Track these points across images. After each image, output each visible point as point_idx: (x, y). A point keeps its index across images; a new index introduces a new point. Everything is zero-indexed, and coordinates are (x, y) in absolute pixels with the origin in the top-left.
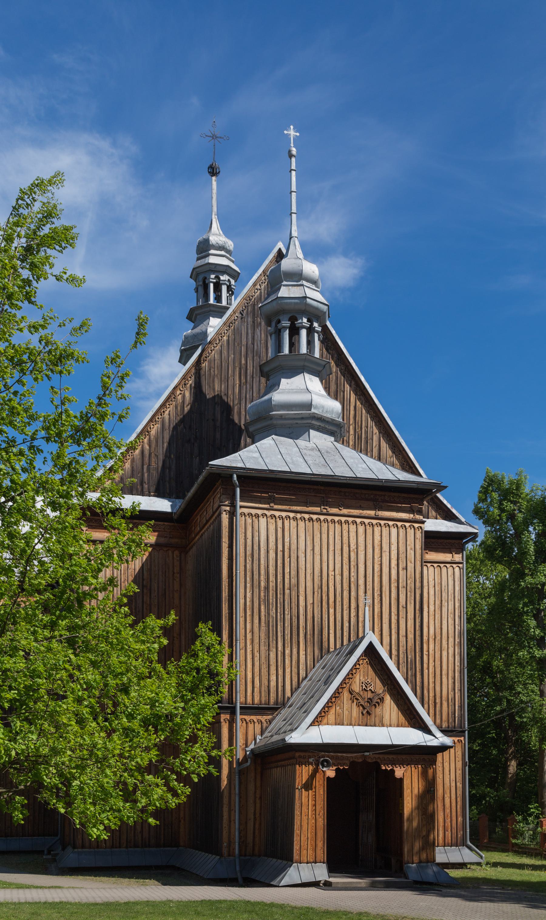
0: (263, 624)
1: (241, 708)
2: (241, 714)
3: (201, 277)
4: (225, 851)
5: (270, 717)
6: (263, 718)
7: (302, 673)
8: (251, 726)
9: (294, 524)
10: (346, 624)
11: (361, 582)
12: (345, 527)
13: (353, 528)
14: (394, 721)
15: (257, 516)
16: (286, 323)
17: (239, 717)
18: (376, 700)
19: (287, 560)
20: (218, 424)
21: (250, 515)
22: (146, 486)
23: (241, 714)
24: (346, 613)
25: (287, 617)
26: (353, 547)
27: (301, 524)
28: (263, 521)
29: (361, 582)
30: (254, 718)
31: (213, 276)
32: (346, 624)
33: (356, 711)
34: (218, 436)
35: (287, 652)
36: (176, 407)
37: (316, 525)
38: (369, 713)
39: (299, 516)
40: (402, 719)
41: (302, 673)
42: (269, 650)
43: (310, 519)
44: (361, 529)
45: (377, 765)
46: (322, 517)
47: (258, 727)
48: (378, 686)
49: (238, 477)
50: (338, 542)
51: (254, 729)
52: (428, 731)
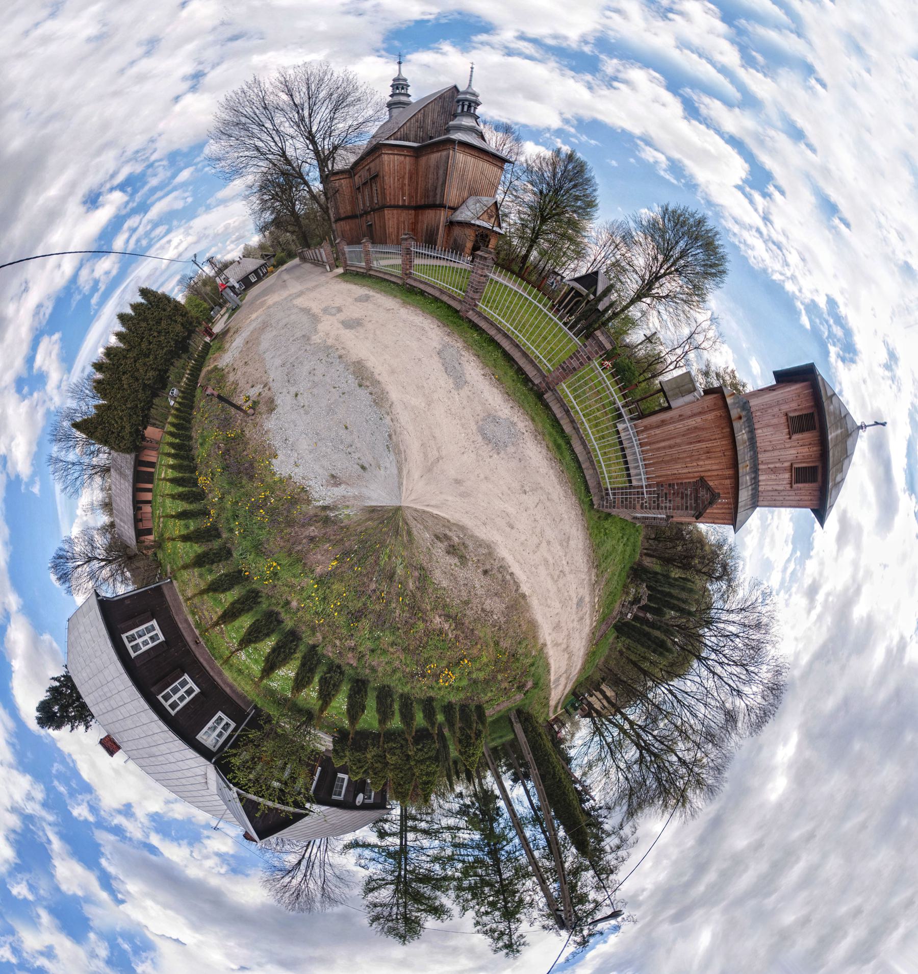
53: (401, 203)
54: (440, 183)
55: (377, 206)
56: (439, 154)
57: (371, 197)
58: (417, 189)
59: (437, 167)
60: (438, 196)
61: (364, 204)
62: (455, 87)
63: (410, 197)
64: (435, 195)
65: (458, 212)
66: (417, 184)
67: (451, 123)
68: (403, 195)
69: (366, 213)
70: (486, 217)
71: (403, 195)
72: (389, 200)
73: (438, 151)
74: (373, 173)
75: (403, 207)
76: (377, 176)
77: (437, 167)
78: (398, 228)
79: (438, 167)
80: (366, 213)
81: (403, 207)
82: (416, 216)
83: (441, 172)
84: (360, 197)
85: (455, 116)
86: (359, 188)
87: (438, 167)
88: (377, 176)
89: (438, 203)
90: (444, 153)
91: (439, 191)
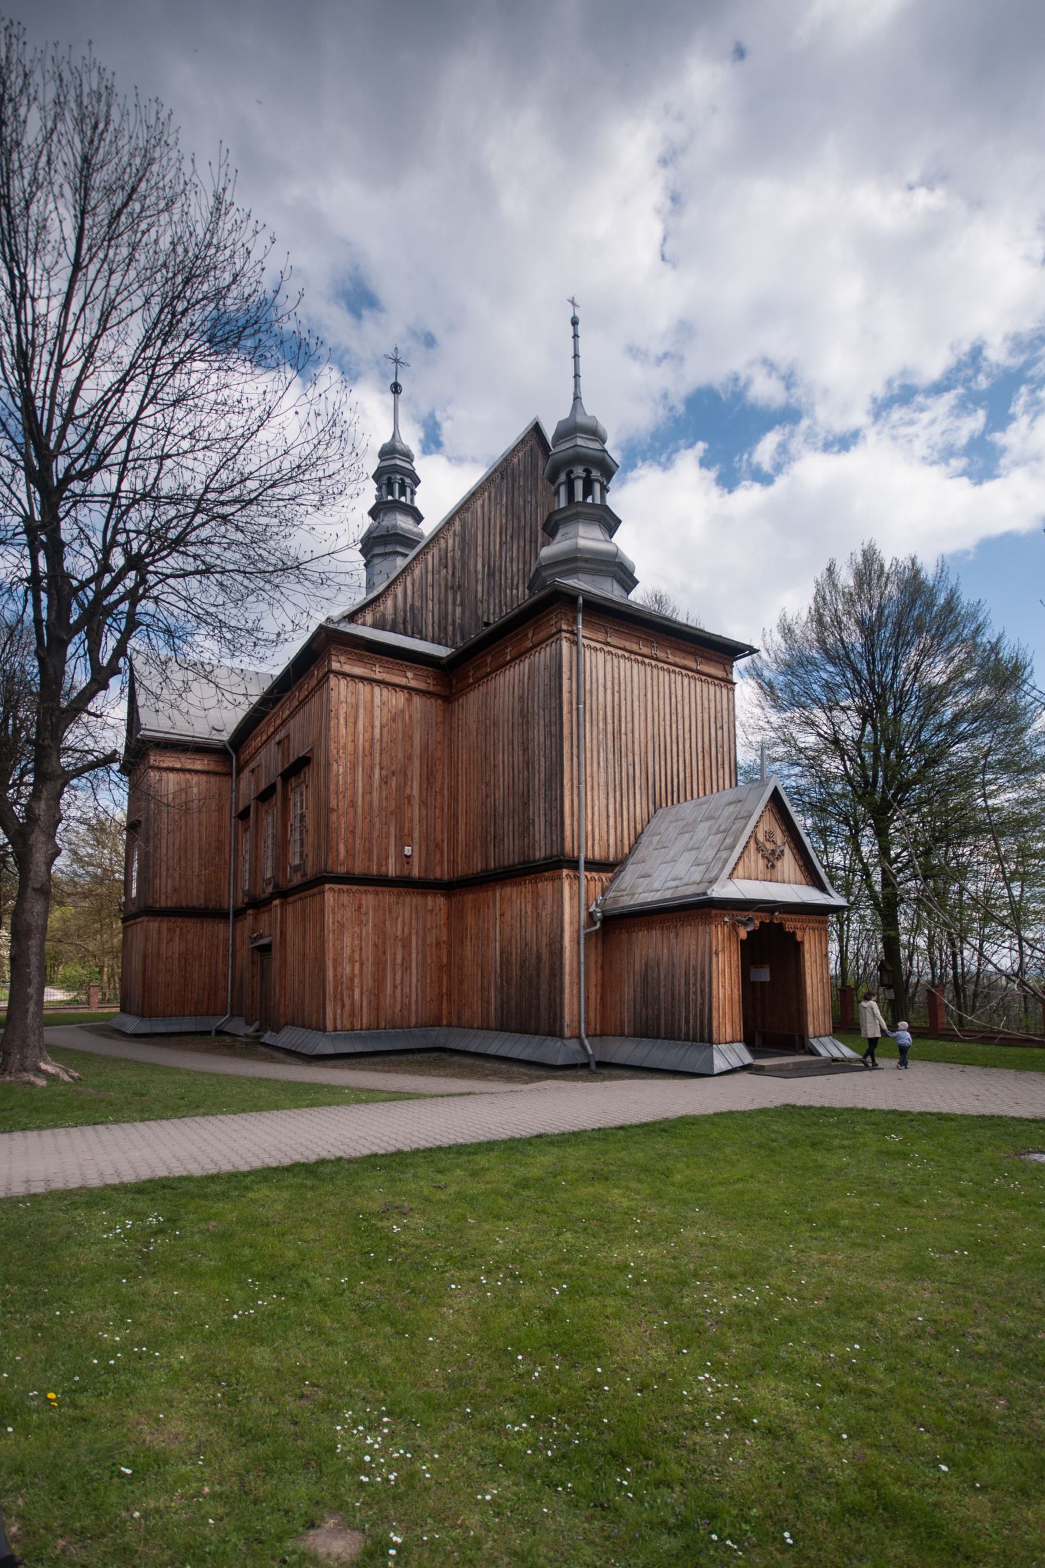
0: (602, 770)
1: (586, 862)
2: (586, 870)
3: (385, 477)
4: (567, 1032)
5: (610, 875)
6: (604, 876)
7: (639, 827)
8: (592, 884)
9: (628, 664)
10: (675, 780)
11: (687, 736)
12: (673, 676)
13: (679, 678)
14: (792, 878)
15: (596, 649)
16: (579, 471)
17: (583, 873)
18: (778, 852)
19: (623, 702)
20: (480, 576)
21: (589, 646)
22: (409, 627)
23: (586, 870)
24: (675, 766)
25: (624, 765)
26: (679, 698)
27: (635, 666)
28: (600, 655)
29: (687, 736)
30: (595, 875)
31: (399, 477)
32: (675, 780)
33: (761, 863)
34: (480, 588)
35: (625, 803)
36: (440, 550)
37: (649, 669)
38: (773, 866)
39: (633, 657)
40: (799, 876)
41: (639, 827)
42: (607, 799)
43: (643, 663)
44: (686, 680)
45: (781, 926)
46: (654, 663)
47: (599, 884)
48: (779, 837)
49: (584, 600)
50: (667, 691)
51: (596, 888)
52: (822, 889)
53: (392, 869)
54: (540, 777)
55: (297, 879)
56: (523, 668)
57: (282, 845)
58: (454, 816)
59: (524, 714)
60: (540, 827)
61: (255, 871)
62: (536, 429)
63: (430, 846)
64: (525, 829)
65: (629, 875)
66: (454, 798)
67: (545, 552)
68: (402, 840)
69: (257, 904)
70: (756, 862)
71: (402, 840)
72: (341, 860)
73: (519, 657)
74: (297, 751)
75: (404, 883)
76: (304, 762)
77: (524, 714)
78: (379, 964)
79: (525, 716)
80: (257, 904)
81: (404, 883)
82: (454, 917)
83: (539, 734)
84: (246, 846)
85: (551, 530)
86: (244, 815)
87: (525, 716)
88: (304, 762)
89: (540, 853)
90: (542, 657)
91: (538, 808)
